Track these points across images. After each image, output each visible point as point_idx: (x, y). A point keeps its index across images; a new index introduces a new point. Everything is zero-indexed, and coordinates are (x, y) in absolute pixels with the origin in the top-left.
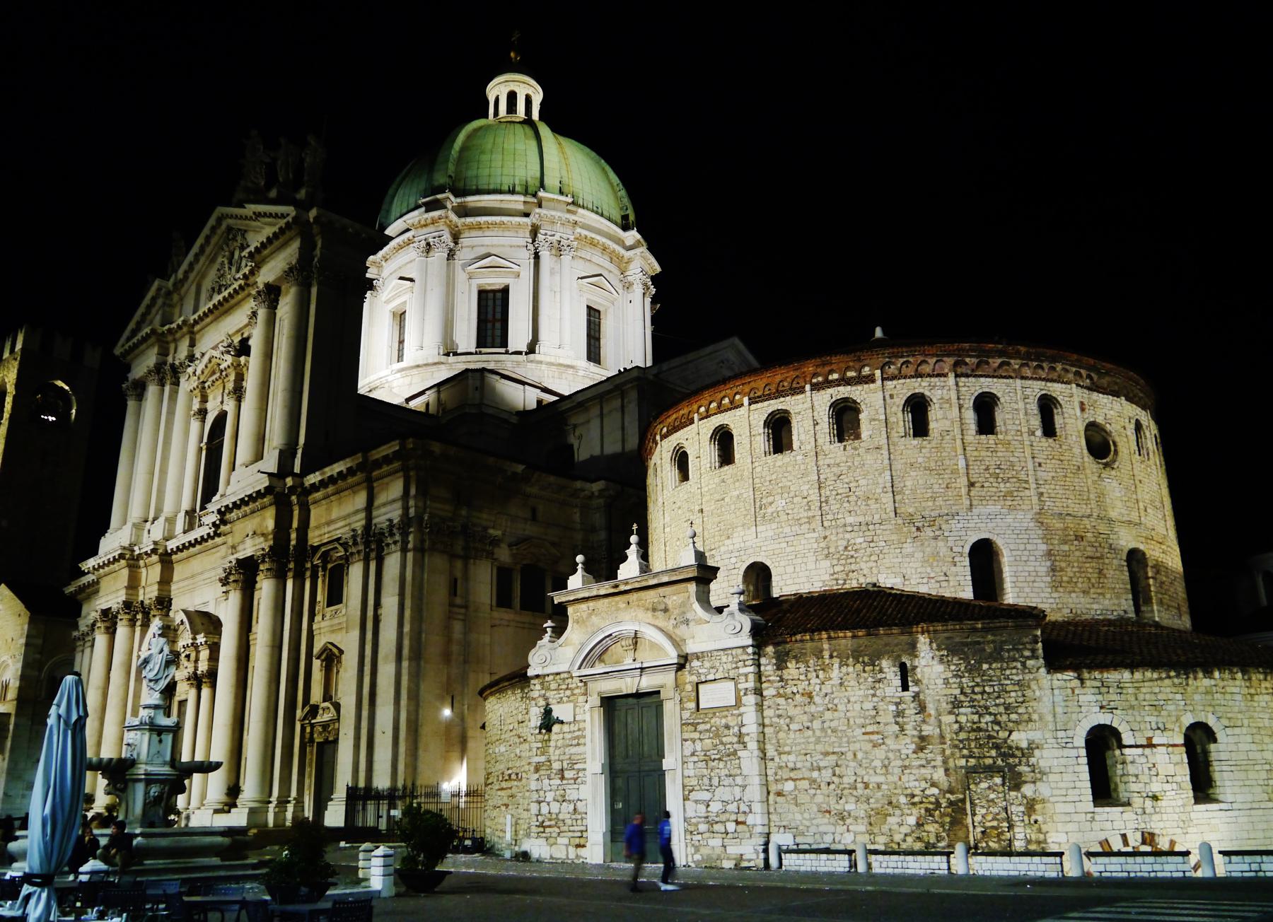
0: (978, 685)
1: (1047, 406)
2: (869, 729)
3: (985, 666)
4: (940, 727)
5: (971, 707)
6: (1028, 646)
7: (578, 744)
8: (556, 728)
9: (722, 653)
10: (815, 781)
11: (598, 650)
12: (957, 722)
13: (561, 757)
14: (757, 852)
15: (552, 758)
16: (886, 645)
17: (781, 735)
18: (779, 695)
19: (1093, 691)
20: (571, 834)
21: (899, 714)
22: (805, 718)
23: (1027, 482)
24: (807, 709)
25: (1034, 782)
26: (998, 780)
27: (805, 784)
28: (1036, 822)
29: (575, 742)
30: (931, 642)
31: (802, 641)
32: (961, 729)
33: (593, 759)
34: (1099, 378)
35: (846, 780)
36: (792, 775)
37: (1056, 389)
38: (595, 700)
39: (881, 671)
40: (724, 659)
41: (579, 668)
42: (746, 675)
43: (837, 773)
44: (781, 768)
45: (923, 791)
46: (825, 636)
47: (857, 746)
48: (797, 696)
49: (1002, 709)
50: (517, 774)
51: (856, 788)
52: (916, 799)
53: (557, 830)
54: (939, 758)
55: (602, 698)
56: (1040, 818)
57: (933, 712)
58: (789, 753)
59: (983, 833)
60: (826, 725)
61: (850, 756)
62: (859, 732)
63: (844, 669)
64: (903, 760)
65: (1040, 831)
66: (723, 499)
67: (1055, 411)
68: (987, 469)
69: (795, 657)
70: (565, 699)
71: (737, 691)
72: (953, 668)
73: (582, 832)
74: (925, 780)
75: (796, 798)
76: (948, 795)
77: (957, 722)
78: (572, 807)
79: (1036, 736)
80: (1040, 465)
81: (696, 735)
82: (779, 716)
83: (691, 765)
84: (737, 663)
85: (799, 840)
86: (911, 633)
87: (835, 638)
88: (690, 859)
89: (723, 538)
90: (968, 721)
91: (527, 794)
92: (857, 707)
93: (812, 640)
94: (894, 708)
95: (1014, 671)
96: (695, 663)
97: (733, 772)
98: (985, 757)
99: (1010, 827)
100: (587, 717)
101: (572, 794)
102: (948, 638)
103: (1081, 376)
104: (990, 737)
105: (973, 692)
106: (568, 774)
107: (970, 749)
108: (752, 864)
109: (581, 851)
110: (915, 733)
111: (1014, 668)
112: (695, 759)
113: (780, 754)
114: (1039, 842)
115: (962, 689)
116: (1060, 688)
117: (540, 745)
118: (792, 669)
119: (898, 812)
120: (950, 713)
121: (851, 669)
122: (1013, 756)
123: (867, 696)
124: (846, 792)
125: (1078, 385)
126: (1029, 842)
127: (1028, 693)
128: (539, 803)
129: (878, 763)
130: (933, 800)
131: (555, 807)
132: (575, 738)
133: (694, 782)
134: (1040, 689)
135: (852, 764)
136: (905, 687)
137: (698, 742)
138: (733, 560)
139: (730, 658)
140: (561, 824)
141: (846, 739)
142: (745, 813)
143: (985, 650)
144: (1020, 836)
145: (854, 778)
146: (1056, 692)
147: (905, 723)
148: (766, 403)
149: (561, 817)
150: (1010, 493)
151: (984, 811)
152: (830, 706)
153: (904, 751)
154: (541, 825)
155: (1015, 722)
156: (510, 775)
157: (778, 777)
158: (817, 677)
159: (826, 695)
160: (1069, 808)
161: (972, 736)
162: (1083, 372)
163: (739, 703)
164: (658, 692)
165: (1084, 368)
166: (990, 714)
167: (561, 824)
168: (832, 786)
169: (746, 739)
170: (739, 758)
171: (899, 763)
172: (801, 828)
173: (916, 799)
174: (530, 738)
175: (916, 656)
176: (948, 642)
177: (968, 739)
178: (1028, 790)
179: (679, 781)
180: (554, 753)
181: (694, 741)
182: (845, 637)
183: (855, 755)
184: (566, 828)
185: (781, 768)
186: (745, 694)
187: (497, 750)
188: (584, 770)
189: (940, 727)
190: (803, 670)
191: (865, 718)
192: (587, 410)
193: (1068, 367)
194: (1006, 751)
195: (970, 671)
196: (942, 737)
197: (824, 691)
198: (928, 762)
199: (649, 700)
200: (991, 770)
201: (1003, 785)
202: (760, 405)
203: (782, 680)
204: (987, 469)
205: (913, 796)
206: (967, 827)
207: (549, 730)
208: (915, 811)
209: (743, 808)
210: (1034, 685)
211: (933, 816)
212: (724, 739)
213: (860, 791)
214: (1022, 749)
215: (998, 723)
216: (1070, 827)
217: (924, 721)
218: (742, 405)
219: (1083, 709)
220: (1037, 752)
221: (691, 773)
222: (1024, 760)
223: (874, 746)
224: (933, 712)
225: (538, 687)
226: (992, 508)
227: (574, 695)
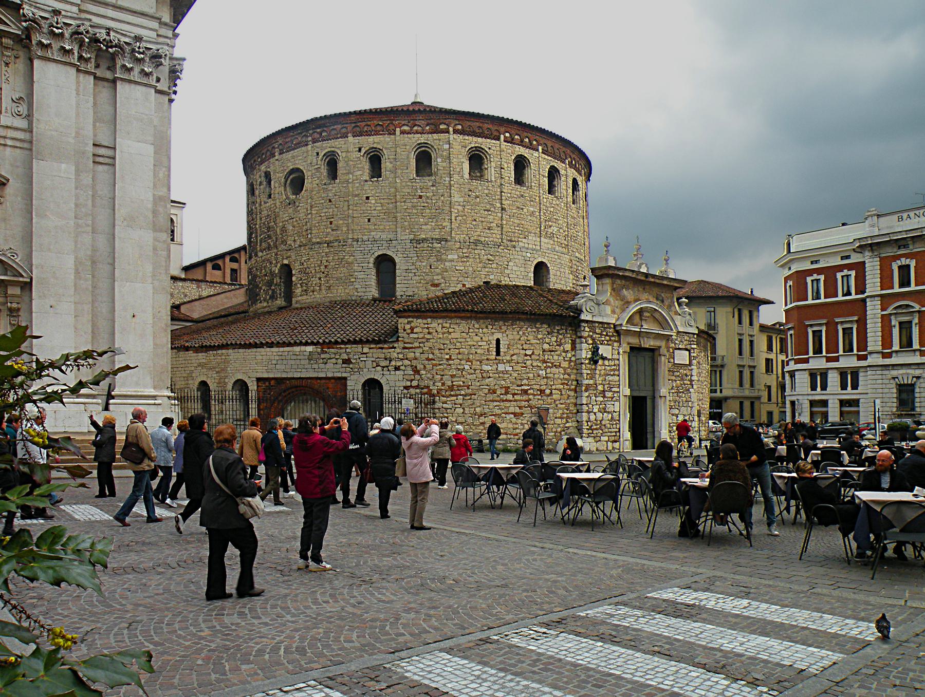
8: (600, 362)
13: (604, 383)
15: (598, 382)
20: (609, 434)
29: (612, 373)
38: (625, 347)
50: (542, 392)
53: (601, 432)
55: (631, 348)
66: (522, 209)
73: (616, 432)
81: (674, 378)
83: (671, 394)
89: (521, 236)
101: (610, 408)
106: (609, 394)
112: (673, 391)
128: (588, 412)
131: (600, 415)
132: (611, 370)
133: (672, 404)
138: (529, 255)
148: (550, 158)
149: (603, 423)
154: (591, 428)
163: (690, 364)
169: (693, 383)
180: (599, 380)
181: (672, 380)
188: (619, 392)
199: (653, 352)
202: (546, 157)
207: (596, 362)
218: (538, 150)
225: (587, 329)
227: (610, 340)
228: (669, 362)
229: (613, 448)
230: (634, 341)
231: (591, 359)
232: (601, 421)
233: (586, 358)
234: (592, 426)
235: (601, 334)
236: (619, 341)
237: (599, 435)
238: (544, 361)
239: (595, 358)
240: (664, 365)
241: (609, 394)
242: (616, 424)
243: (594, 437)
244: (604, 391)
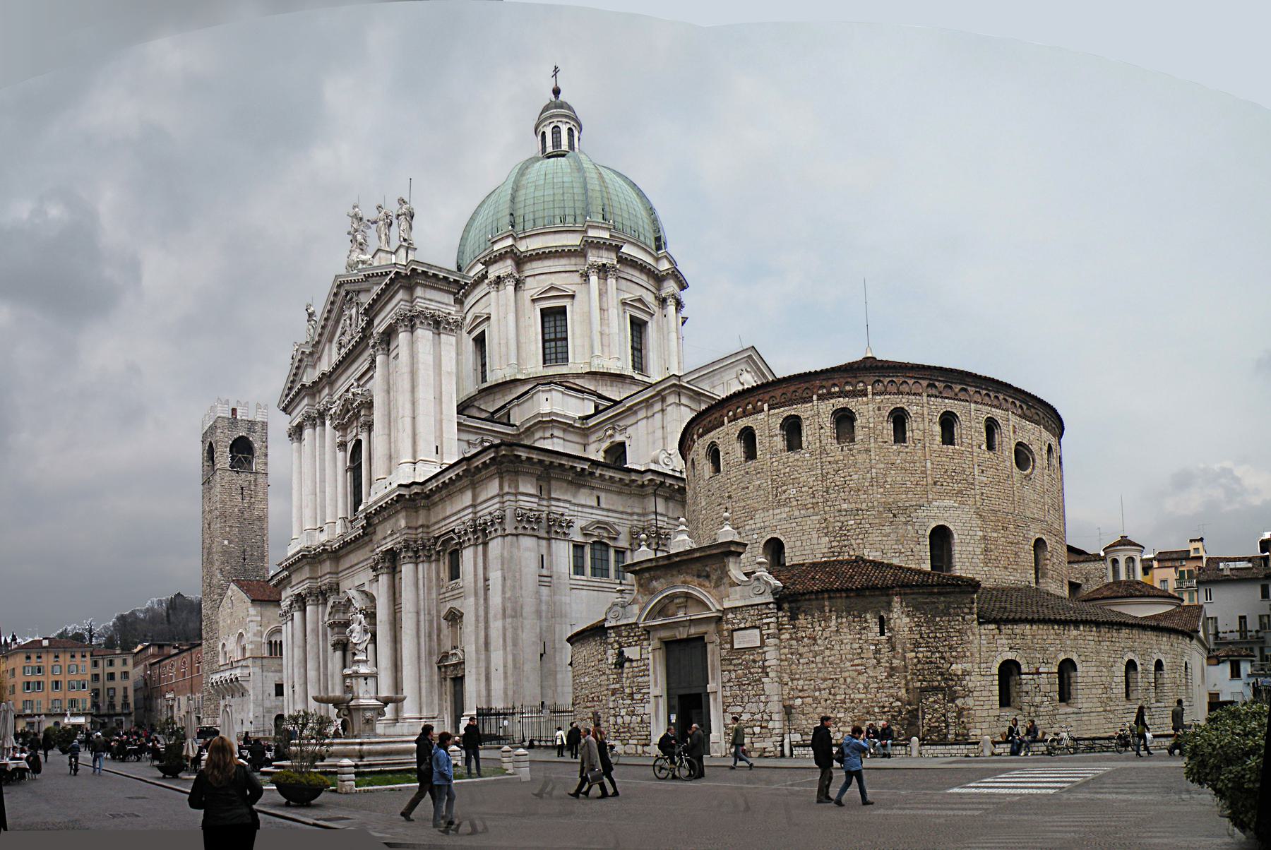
0: (932, 632)
1: (991, 426)
2: (856, 662)
3: (938, 619)
4: (904, 661)
5: (926, 647)
6: (968, 606)
7: (644, 675)
8: (627, 665)
9: (750, 608)
10: (817, 698)
11: (658, 609)
12: (916, 657)
14: (775, 746)
16: (871, 603)
17: (794, 667)
18: (791, 638)
19: (1007, 637)
20: (639, 737)
21: (877, 651)
22: (811, 655)
23: (972, 484)
24: (812, 648)
25: (964, 698)
26: (940, 696)
27: (809, 700)
28: (963, 722)
29: (642, 674)
30: (901, 602)
31: (809, 600)
32: (919, 662)
33: (656, 685)
34: (1027, 409)
35: (838, 697)
36: (800, 694)
37: (998, 414)
38: (655, 643)
39: (866, 621)
40: (752, 612)
41: (645, 620)
42: (768, 624)
43: (832, 692)
44: (793, 689)
45: (891, 704)
46: (826, 596)
47: (847, 674)
48: (805, 639)
49: (947, 649)
50: (598, 697)
51: (845, 703)
52: (886, 709)
53: (629, 735)
54: (903, 682)
56: (965, 720)
57: (900, 651)
58: (798, 679)
59: (928, 730)
60: (826, 659)
61: (842, 680)
62: (848, 664)
63: (839, 621)
64: (878, 683)
65: (964, 728)
67: (996, 431)
68: (946, 472)
69: (804, 611)
70: (633, 643)
71: (762, 636)
72: (916, 619)
73: (647, 735)
74: (892, 696)
75: (803, 710)
76: (907, 707)
77: (916, 657)
78: (639, 719)
79: (968, 666)
80: (983, 472)
81: (732, 667)
82: (792, 654)
84: (761, 615)
85: (805, 737)
86: (888, 595)
87: (834, 598)
88: (728, 752)
90: (924, 657)
91: (607, 710)
92: (848, 647)
93: (817, 599)
94: (874, 647)
95: (957, 623)
96: (730, 616)
97: (759, 693)
98: (934, 681)
99: (947, 727)
100: (651, 656)
101: (639, 710)
102: (913, 599)
103: (1016, 406)
104: (938, 668)
105: (929, 637)
106: (637, 696)
107: (923, 675)
108: (772, 754)
109: (646, 749)
110: (887, 665)
111: (958, 620)
112: (731, 684)
113: (792, 680)
114: (963, 735)
115: (921, 634)
116: (986, 635)
117: (615, 676)
118: (802, 621)
119: (873, 718)
120: (912, 651)
121: (844, 620)
122: (952, 680)
123: (855, 639)
124: (838, 705)
125: (1013, 413)
126: (957, 735)
127: (965, 638)
128: (615, 716)
129: (861, 686)
130: (896, 709)
131: (627, 719)
132: (640, 671)
134: (974, 634)
135: (843, 686)
136: (882, 633)
137: (733, 672)
139: (756, 612)
140: (632, 731)
141: (839, 670)
142: (766, 720)
143: (938, 608)
144: (951, 732)
145: (843, 696)
146: (983, 637)
147: (881, 658)
149: (632, 726)
150: (960, 492)
151: (930, 716)
152: (829, 646)
153: (881, 677)
154: (617, 731)
155: (955, 657)
156: (593, 698)
157: (791, 696)
158: (820, 625)
159: (826, 638)
160: (985, 714)
161: (926, 667)
162: (1018, 403)
163: (763, 644)
164: (703, 638)
165: (1018, 400)
166: (939, 652)
167: (632, 731)
168: (829, 702)
169: (768, 670)
170: (763, 683)
171: (876, 685)
172: (806, 730)
173: (886, 709)
174: (607, 672)
175: (891, 611)
176: (913, 601)
177: (923, 669)
178: (959, 702)
179: (720, 699)
180: (626, 682)
182: (841, 597)
183: (845, 680)
184: (636, 733)
185: (793, 689)
186: (768, 638)
187: (582, 680)
188: (649, 693)
189: (904, 661)
190: (809, 620)
191: (853, 654)
192: (636, 412)
193: (1007, 398)
194: (948, 676)
195: (927, 622)
196: (906, 667)
197: (825, 635)
198: (895, 685)
199: (700, 640)
200: (937, 689)
201: (944, 699)
203: (794, 627)
204: (946, 472)
205: (884, 707)
206: (919, 727)
207: (622, 666)
208: (884, 717)
209: (766, 717)
210: (969, 633)
211: (896, 720)
212: (752, 670)
213: (848, 705)
214: (958, 676)
215: (944, 658)
216: (985, 725)
217: (894, 657)
219: (1000, 649)
220: (967, 678)
221: (728, 694)
222: (959, 682)
223: (859, 674)
224: (900, 651)
225: (613, 635)
226: (947, 502)
227: (639, 640)
228: (722, 649)
229: (643, 752)
230: (665, 634)
231: (616, 664)
232: (629, 724)
233: (612, 664)
234: (619, 729)
235: (628, 636)
236: (648, 639)
237: (627, 738)
238: (600, 671)
239: (621, 661)
240: (714, 655)
241: (637, 696)
242: (647, 727)
243: (622, 740)
244: (632, 694)
